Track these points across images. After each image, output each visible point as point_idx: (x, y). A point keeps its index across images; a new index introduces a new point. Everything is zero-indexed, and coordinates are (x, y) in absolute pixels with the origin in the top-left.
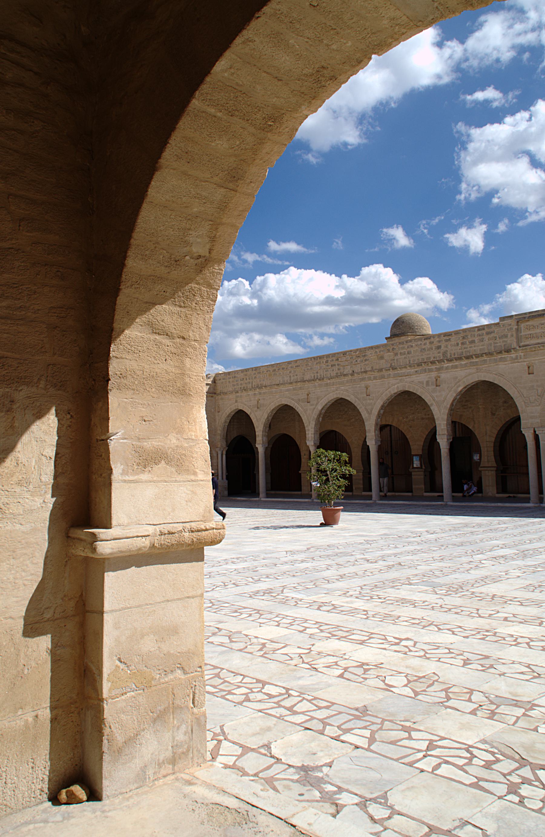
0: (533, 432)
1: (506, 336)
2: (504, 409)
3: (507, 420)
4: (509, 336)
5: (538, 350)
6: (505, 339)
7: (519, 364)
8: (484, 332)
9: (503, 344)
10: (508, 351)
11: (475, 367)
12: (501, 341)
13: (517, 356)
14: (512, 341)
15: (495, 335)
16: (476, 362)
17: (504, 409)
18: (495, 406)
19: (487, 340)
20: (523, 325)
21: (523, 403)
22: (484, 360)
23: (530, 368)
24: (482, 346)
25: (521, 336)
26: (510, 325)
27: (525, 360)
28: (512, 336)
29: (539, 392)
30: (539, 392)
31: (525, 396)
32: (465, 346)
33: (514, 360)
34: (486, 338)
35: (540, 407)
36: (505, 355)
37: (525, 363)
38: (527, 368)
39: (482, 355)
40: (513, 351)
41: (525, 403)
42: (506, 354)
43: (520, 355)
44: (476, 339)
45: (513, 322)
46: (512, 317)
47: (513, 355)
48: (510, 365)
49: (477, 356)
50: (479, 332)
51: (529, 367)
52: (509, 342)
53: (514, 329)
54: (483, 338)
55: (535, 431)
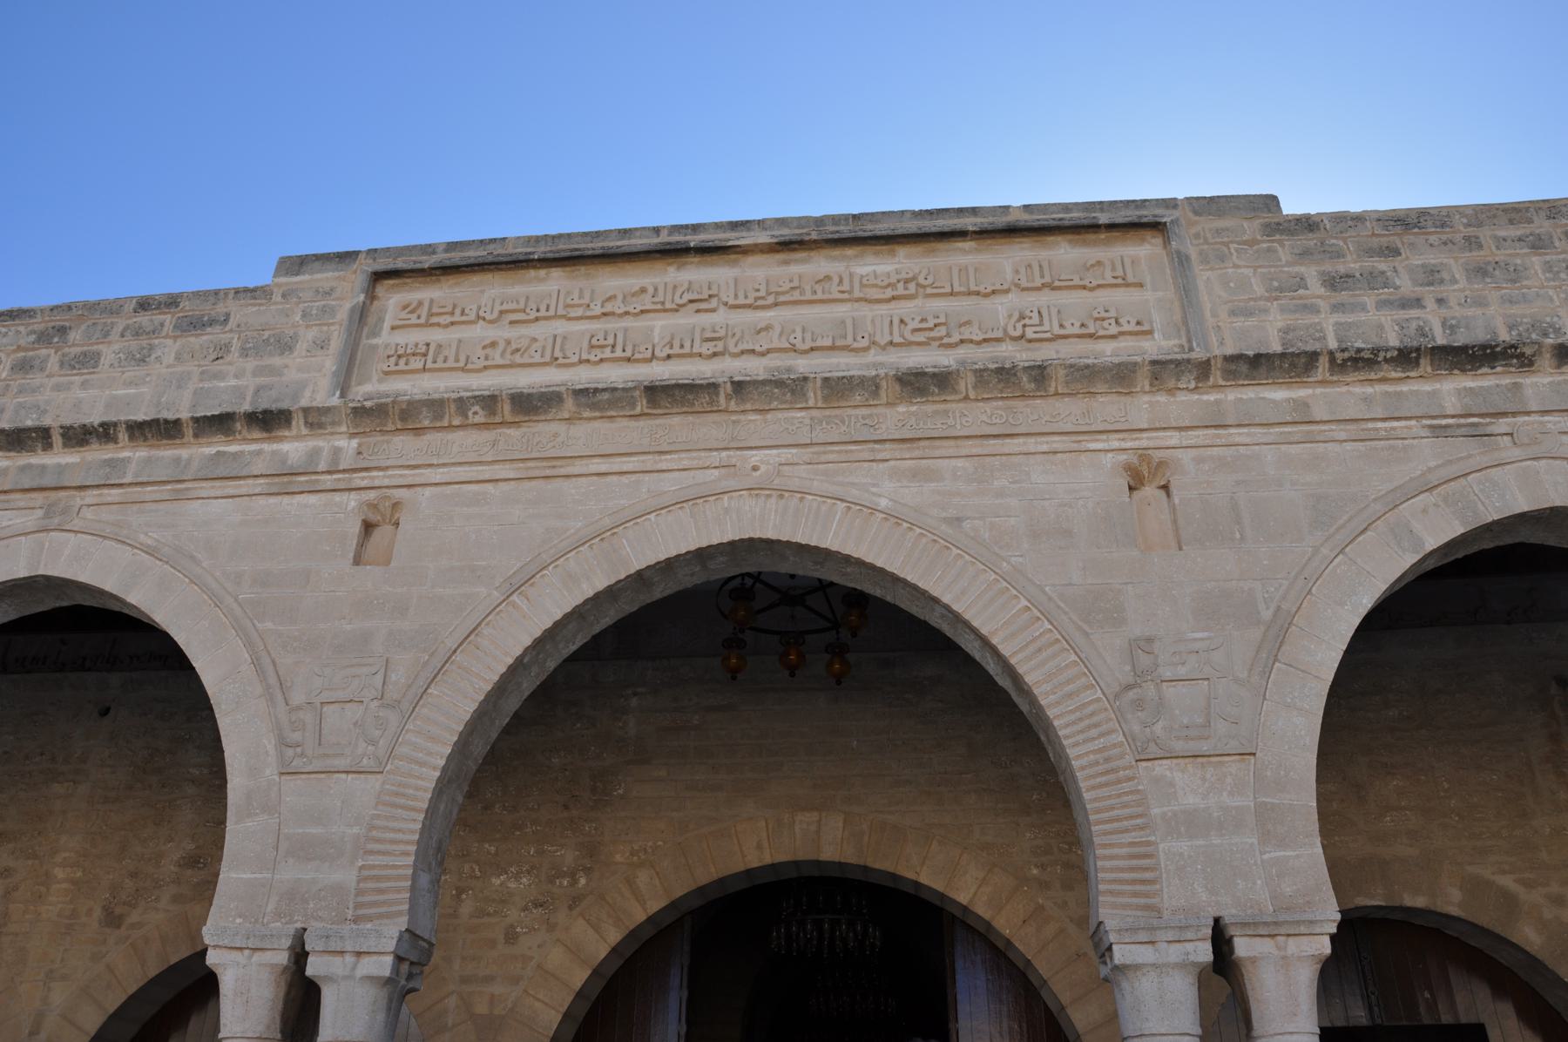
0: (282, 958)
1: (285, 346)
2: (176, 899)
3: (174, 960)
4: (301, 347)
5: (450, 427)
6: (277, 361)
7: (312, 499)
8: (168, 319)
9: (250, 382)
10: (269, 421)
11: (39, 498)
12: (250, 364)
13: (314, 454)
14: (309, 377)
15: (225, 337)
16: (61, 469)
17: (176, 899)
18: (134, 875)
19: (169, 359)
20: (393, 299)
21: (269, 744)
22: (110, 463)
23: (377, 535)
24: (130, 384)
25: (374, 348)
26: (328, 293)
27: (359, 480)
28: (322, 345)
29: (398, 676)
30: (398, 676)
31: (298, 698)
32: (36, 379)
33: (286, 480)
34: (168, 349)
35: (374, 782)
36: (249, 448)
37: (352, 500)
38: (355, 528)
39: (105, 433)
40: (298, 422)
41: (282, 743)
42: (257, 434)
43: (337, 452)
44: (109, 353)
45: (349, 287)
46: (345, 258)
47: (292, 447)
48: (262, 501)
49: (78, 436)
50: (144, 319)
51: (368, 527)
52: (292, 375)
53: (343, 314)
54: (151, 348)
55: (300, 956)
